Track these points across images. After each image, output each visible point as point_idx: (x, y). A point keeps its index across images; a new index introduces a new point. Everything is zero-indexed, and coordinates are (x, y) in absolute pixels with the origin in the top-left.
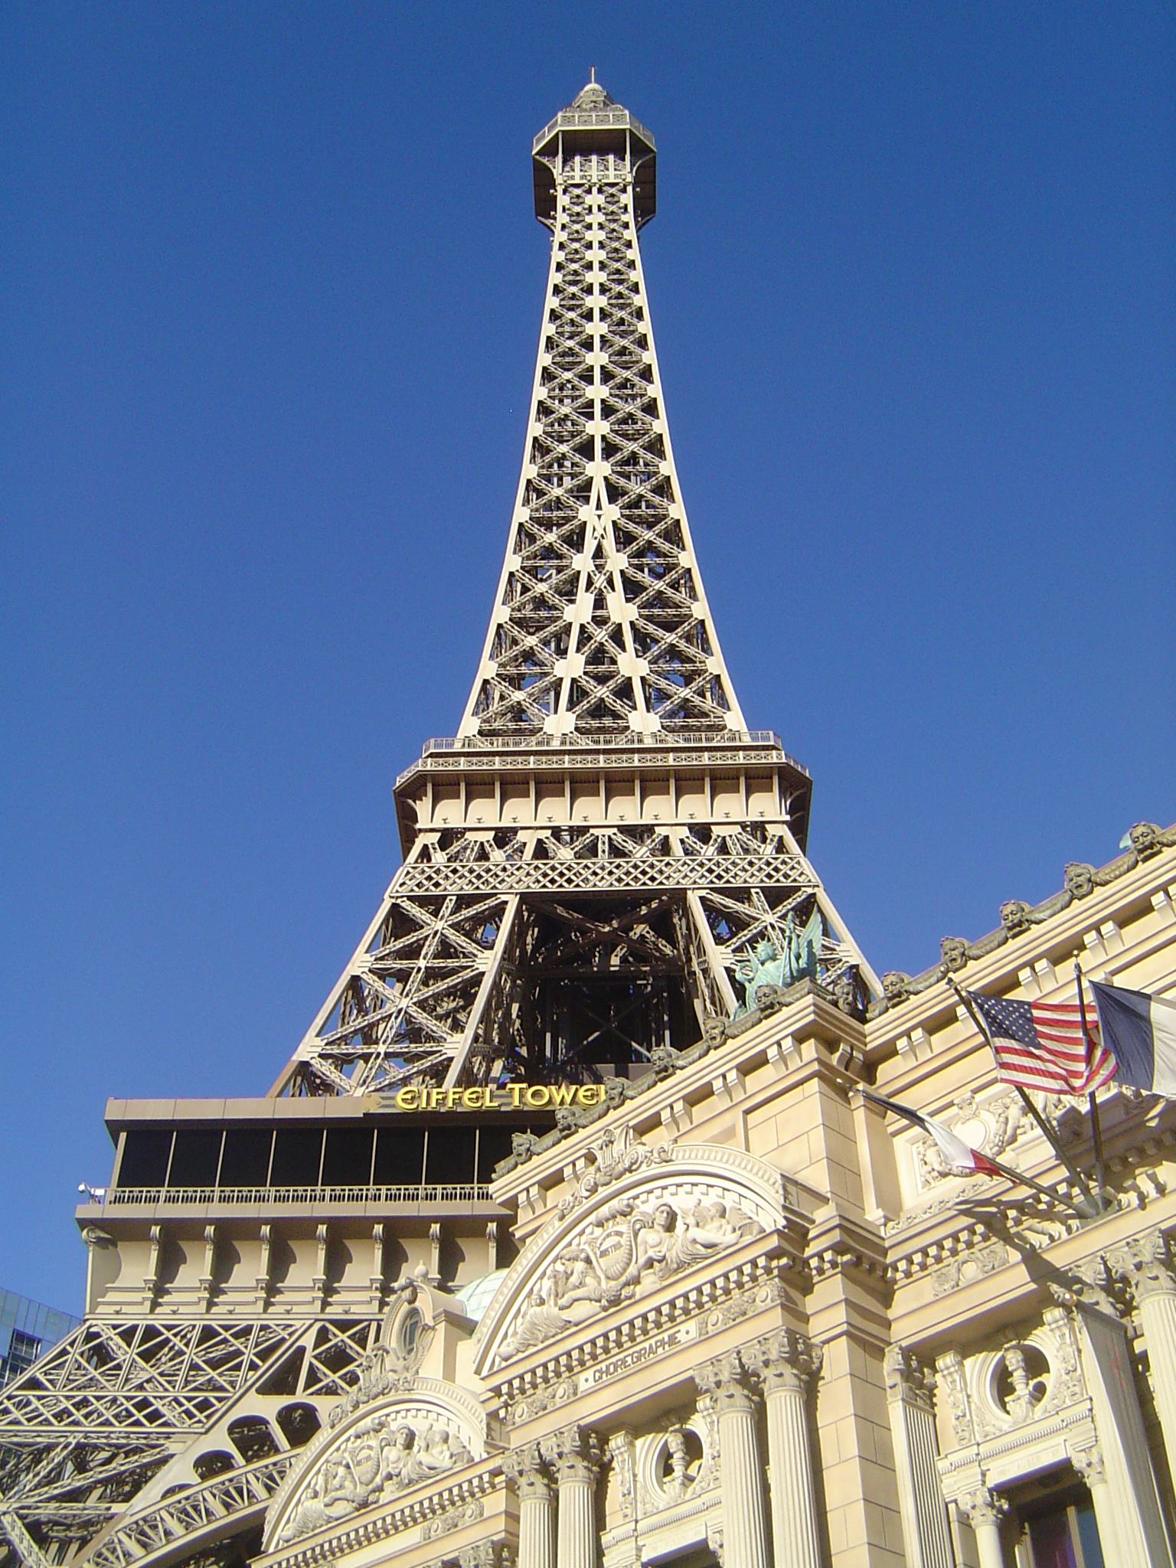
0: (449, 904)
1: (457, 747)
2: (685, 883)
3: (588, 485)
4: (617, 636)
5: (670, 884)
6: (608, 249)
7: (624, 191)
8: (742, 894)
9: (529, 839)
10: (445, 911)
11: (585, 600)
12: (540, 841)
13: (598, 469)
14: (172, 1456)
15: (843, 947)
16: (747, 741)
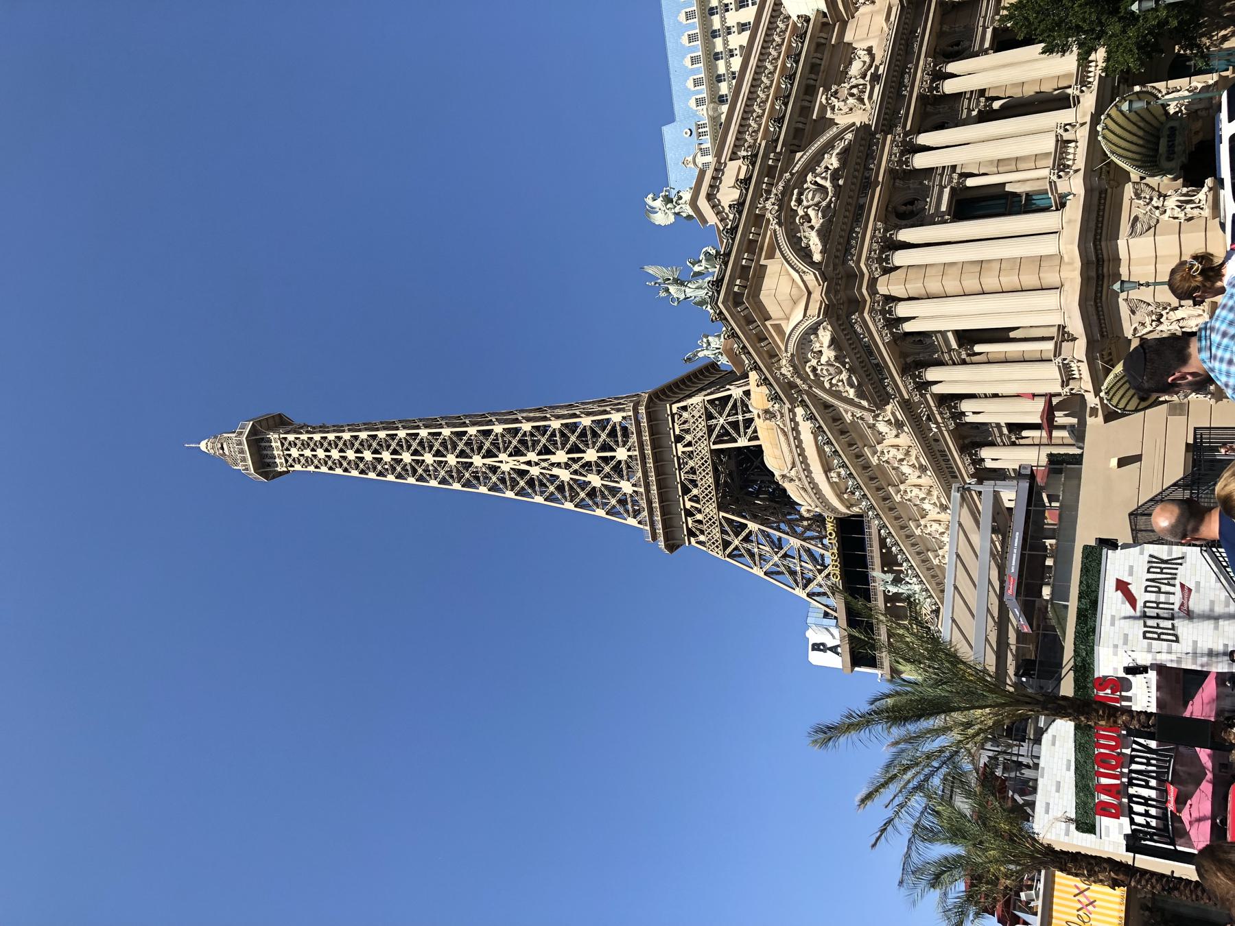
0: (725, 537)
4: (575, 460)
5: (708, 455)
7: (285, 439)
8: (710, 430)
9: (688, 505)
10: (729, 539)
11: (555, 471)
13: (477, 461)
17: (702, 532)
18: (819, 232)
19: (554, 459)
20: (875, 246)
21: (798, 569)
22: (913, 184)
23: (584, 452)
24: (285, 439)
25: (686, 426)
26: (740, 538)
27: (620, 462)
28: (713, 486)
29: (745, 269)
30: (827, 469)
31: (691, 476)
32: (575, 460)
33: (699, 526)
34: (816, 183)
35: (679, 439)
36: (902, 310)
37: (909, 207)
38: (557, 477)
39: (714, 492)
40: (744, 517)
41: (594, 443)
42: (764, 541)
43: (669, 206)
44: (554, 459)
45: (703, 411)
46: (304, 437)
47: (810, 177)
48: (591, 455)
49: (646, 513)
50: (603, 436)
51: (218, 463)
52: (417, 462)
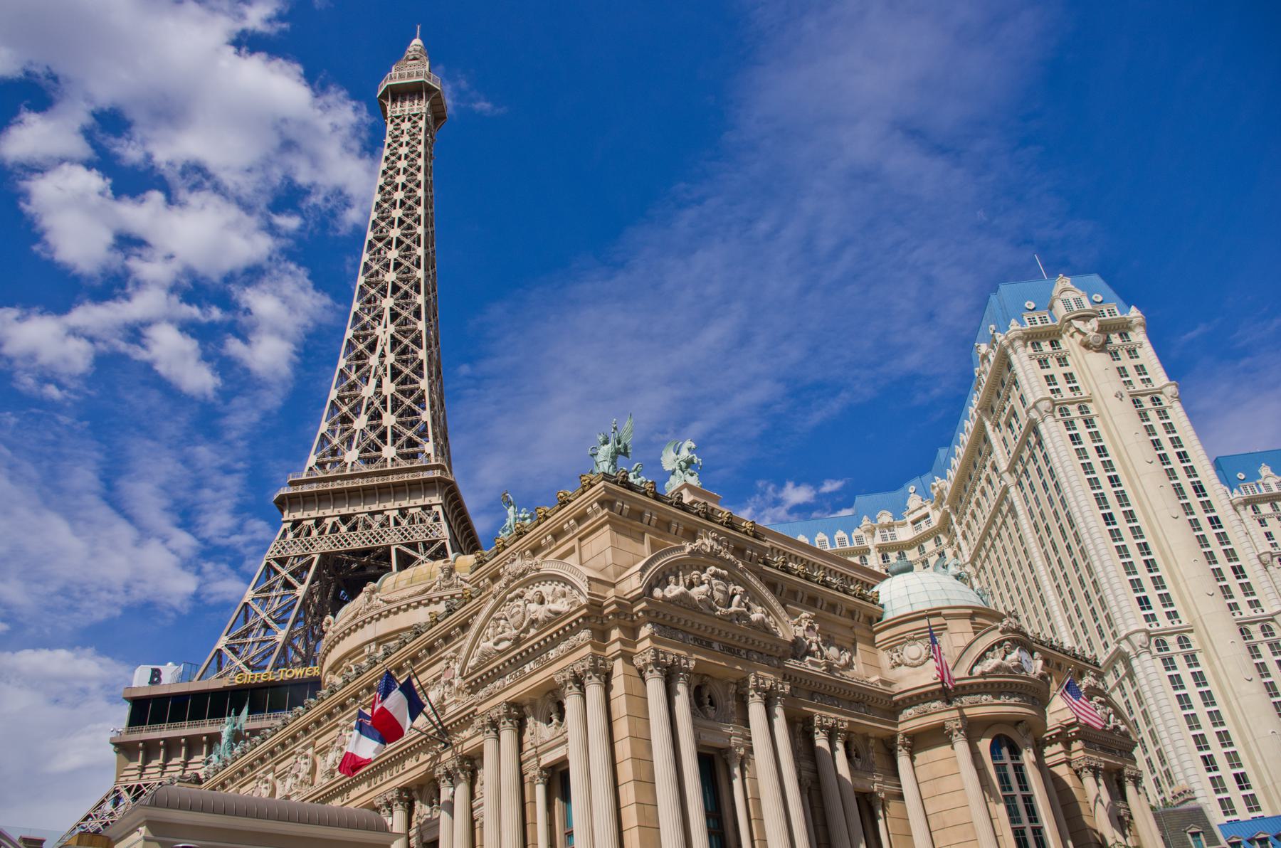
2: (391, 542)
4: (384, 402)
5: (384, 543)
8: (414, 546)
9: (329, 522)
10: (288, 565)
13: (388, 303)
17: (297, 536)
18: (684, 595)
19: (386, 381)
20: (670, 659)
21: (251, 640)
22: (732, 704)
23: (393, 412)
25: (417, 520)
26: (289, 577)
27: (379, 449)
28: (349, 548)
29: (639, 515)
30: (379, 640)
31: (360, 525)
33: (304, 533)
34: (734, 595)
35: (403, 512)
36: (594, 691)
37: (707, 701)
39: (342, 548)
40: (312, 582)
41: (402, 424)
42: (284, 602)
43: (683, 464)
44: (386, 381)
45: (434, 538)
46: (422, 137)
47: (739, 589)
48: (389, 420)
49: (321, 475)
50: (409, 433)
51: (397, 54)
52: (390, 243)
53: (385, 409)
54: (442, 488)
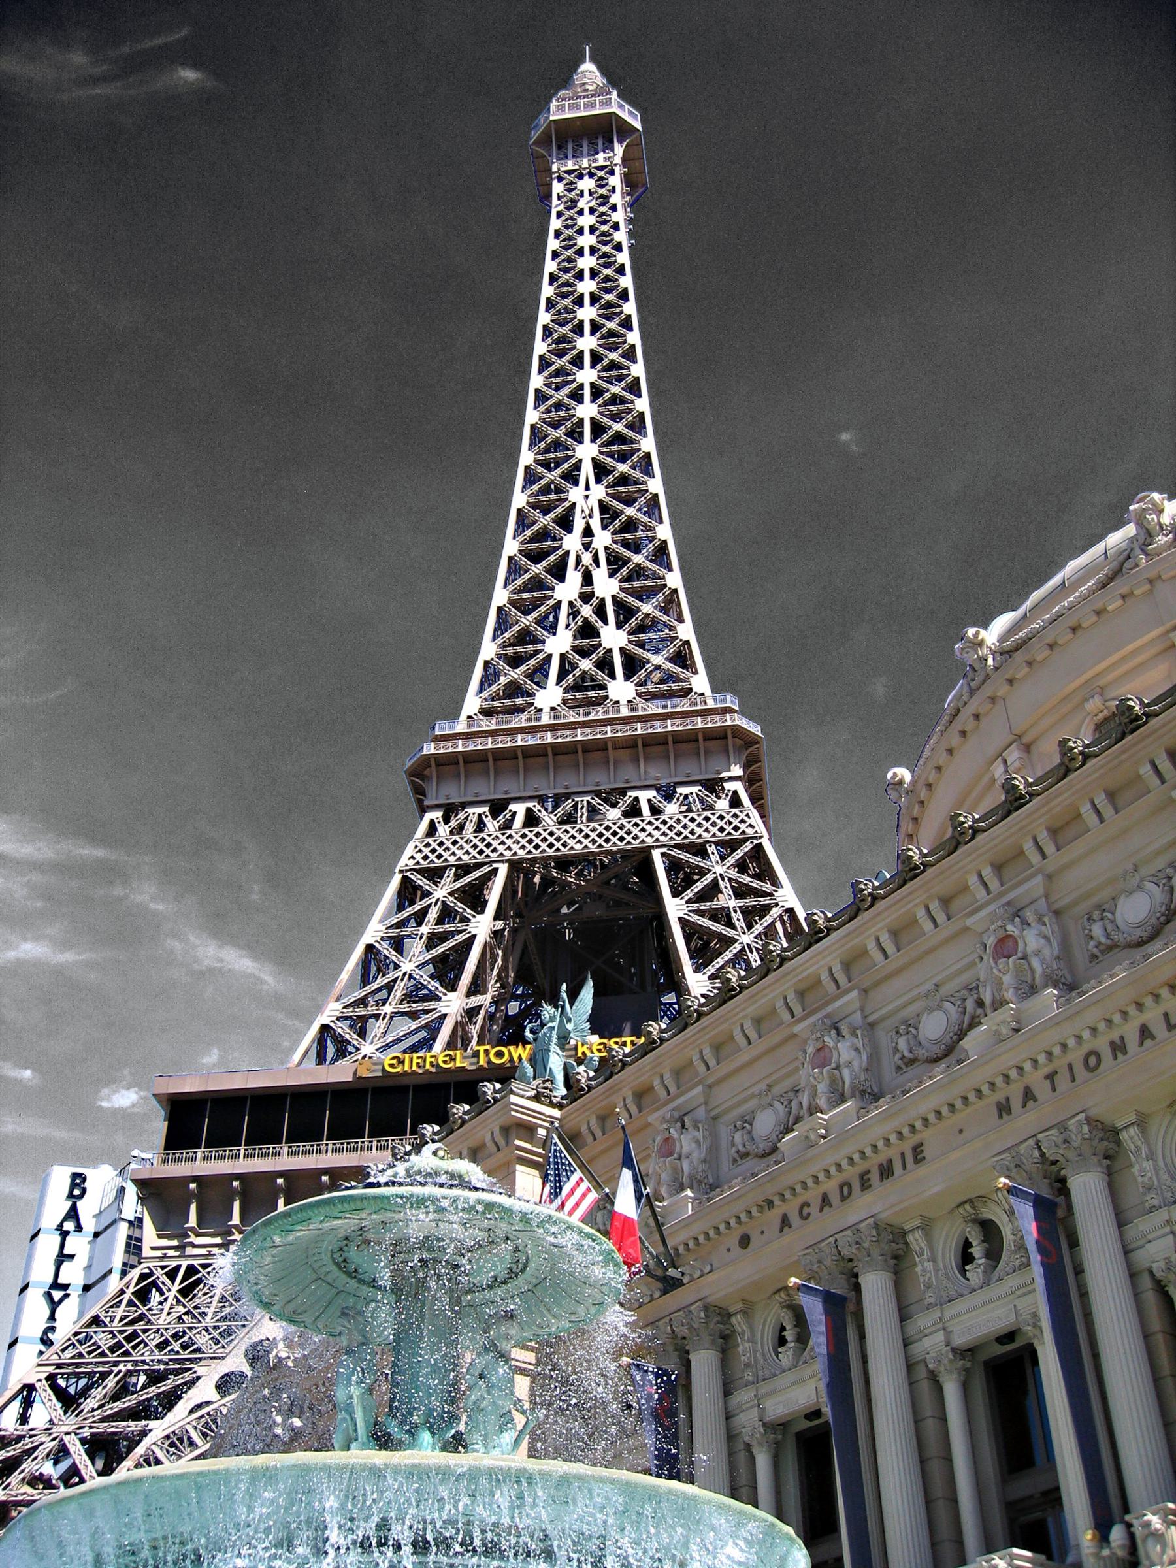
1: (461, 727)
3: (577, 466)
4: (601, 612)
6: (598, 233)
7: (612, 172)
11: (574, 577)
12: (529, 810)
13: (587, 451)
14: (199, 1378)
15: (780, 892)
16: (711, 704)
23: (619, 626)
24: (612, 172)
32: (601, 612)
33: (470, 827)
38: (561, 578)
48: (613, 638)
51: (564, 77)
53: (606, 622)
54: (739, 750)
